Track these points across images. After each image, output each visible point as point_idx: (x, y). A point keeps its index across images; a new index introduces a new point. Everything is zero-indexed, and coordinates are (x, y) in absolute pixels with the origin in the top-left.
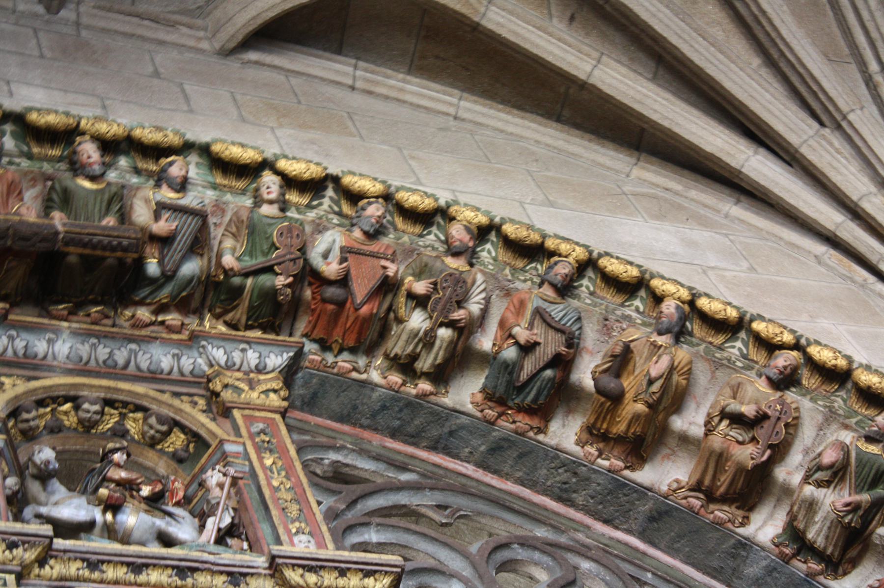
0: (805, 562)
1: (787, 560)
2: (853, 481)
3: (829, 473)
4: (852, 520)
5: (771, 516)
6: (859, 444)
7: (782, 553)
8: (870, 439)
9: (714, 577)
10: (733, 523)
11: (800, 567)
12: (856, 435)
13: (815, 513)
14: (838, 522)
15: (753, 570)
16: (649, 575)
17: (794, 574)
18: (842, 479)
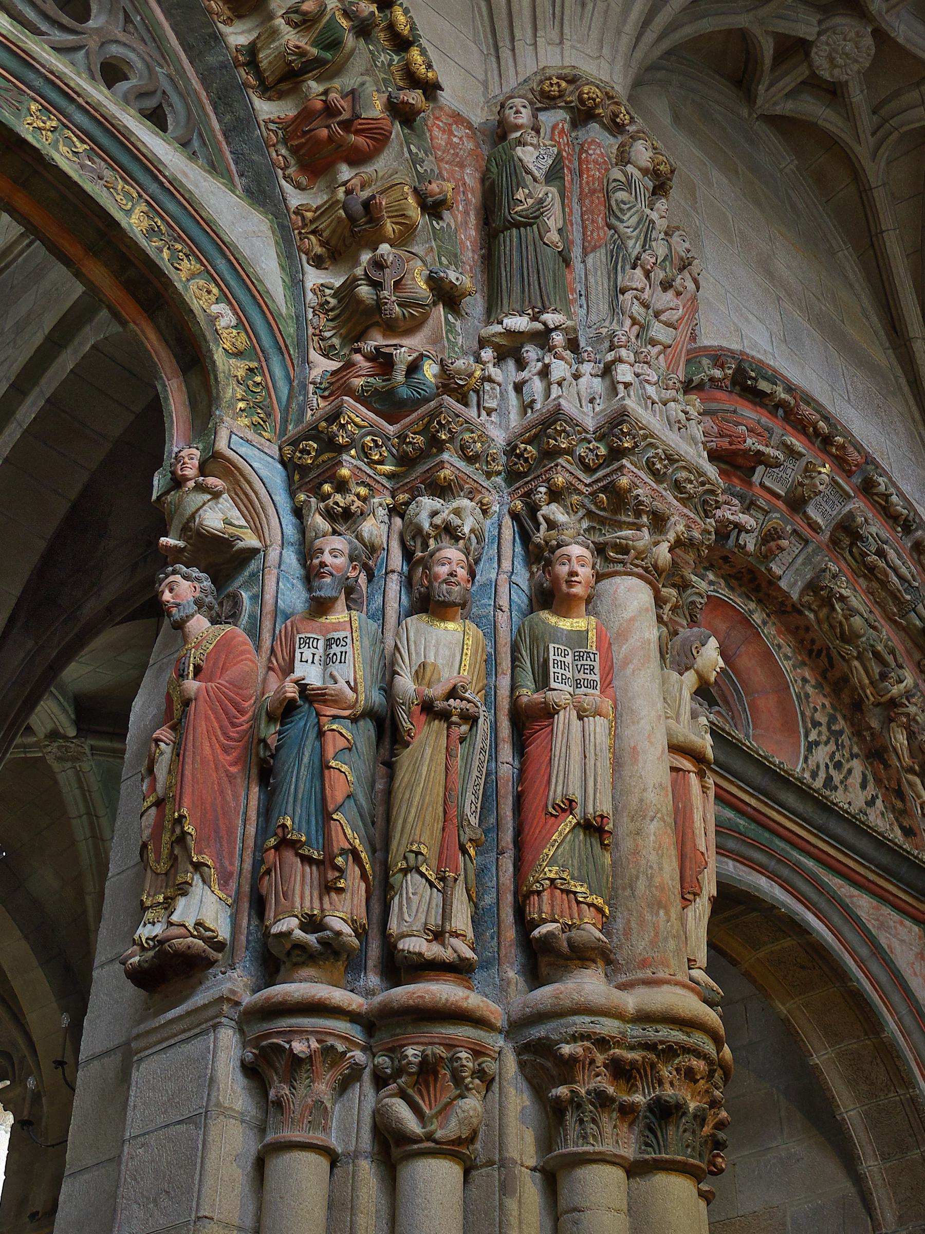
0: (247, 74)
1: (237, 64)
2: (315, 35)
3: (301, 18)
4: (295, 60)
5: (249, 31)
6: (337, 13)
7: (237, 57)
8: (346, 14)
9: (185, 50)
10: (219, 17)
11: (243, 74)
12: (340, 6)
13: (274, 41)
14: (282, 56)
15: (212, 60)
16: (139, 18)
17: (235, 77)
18: (308, 29)
